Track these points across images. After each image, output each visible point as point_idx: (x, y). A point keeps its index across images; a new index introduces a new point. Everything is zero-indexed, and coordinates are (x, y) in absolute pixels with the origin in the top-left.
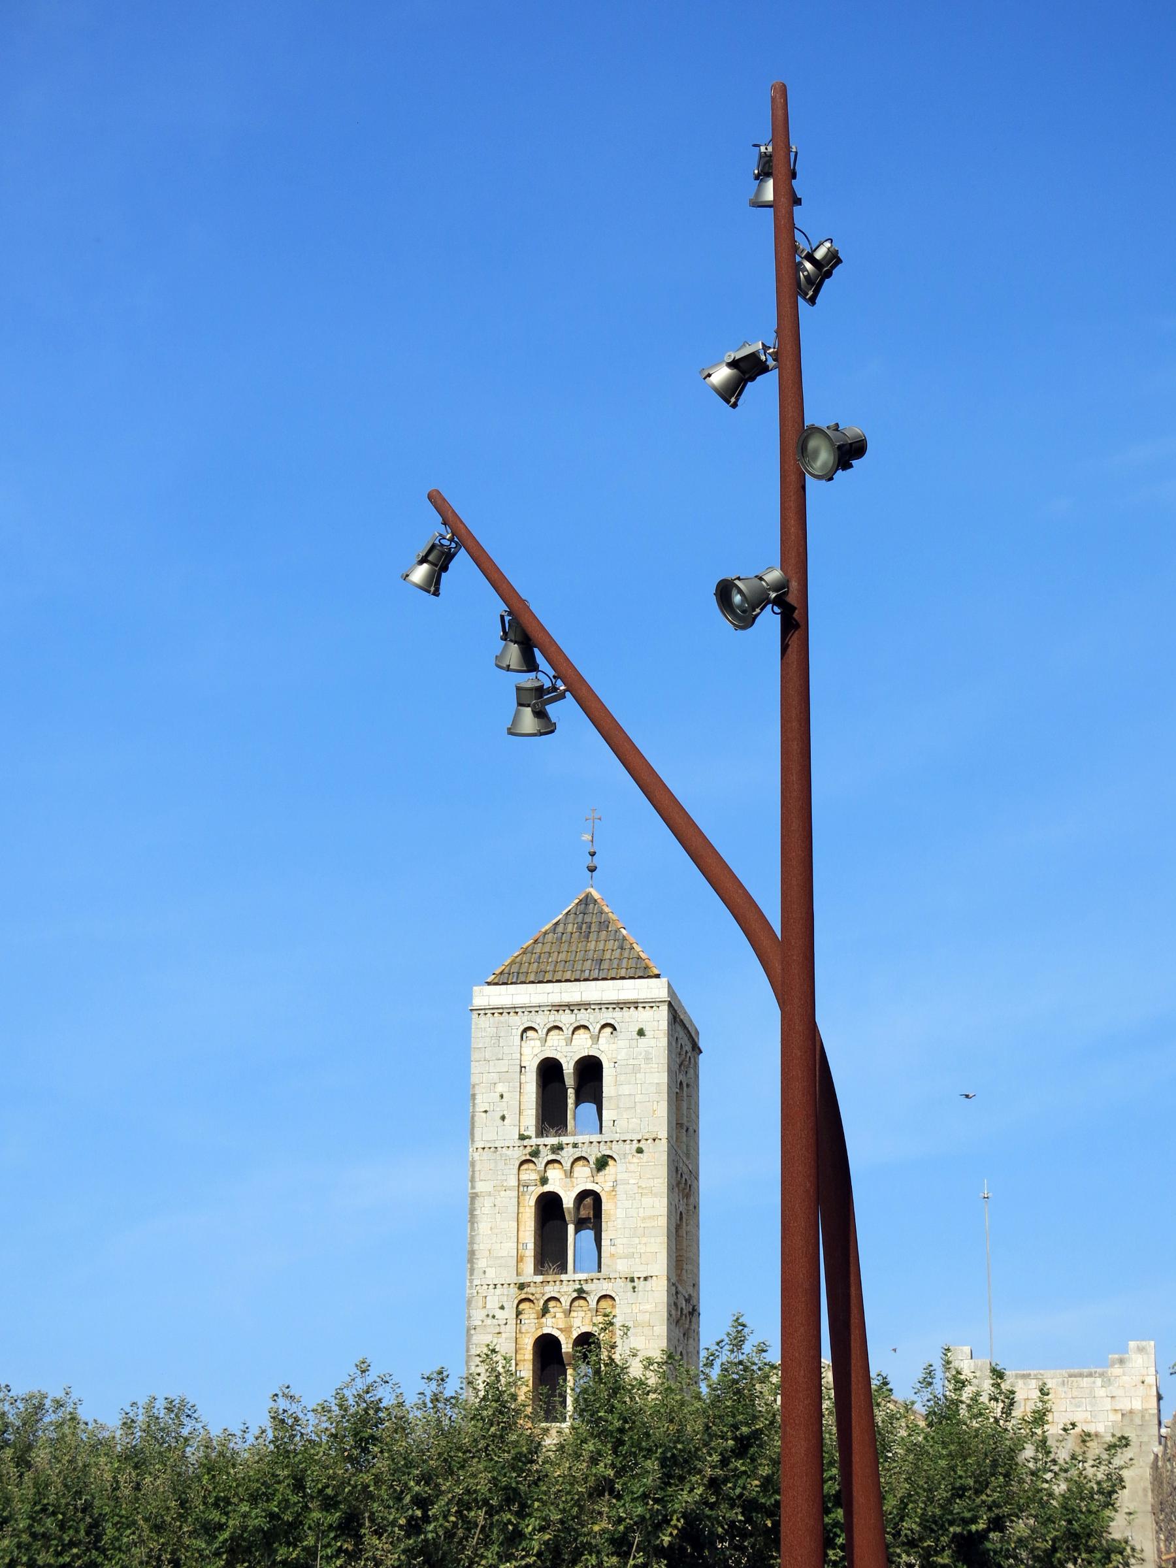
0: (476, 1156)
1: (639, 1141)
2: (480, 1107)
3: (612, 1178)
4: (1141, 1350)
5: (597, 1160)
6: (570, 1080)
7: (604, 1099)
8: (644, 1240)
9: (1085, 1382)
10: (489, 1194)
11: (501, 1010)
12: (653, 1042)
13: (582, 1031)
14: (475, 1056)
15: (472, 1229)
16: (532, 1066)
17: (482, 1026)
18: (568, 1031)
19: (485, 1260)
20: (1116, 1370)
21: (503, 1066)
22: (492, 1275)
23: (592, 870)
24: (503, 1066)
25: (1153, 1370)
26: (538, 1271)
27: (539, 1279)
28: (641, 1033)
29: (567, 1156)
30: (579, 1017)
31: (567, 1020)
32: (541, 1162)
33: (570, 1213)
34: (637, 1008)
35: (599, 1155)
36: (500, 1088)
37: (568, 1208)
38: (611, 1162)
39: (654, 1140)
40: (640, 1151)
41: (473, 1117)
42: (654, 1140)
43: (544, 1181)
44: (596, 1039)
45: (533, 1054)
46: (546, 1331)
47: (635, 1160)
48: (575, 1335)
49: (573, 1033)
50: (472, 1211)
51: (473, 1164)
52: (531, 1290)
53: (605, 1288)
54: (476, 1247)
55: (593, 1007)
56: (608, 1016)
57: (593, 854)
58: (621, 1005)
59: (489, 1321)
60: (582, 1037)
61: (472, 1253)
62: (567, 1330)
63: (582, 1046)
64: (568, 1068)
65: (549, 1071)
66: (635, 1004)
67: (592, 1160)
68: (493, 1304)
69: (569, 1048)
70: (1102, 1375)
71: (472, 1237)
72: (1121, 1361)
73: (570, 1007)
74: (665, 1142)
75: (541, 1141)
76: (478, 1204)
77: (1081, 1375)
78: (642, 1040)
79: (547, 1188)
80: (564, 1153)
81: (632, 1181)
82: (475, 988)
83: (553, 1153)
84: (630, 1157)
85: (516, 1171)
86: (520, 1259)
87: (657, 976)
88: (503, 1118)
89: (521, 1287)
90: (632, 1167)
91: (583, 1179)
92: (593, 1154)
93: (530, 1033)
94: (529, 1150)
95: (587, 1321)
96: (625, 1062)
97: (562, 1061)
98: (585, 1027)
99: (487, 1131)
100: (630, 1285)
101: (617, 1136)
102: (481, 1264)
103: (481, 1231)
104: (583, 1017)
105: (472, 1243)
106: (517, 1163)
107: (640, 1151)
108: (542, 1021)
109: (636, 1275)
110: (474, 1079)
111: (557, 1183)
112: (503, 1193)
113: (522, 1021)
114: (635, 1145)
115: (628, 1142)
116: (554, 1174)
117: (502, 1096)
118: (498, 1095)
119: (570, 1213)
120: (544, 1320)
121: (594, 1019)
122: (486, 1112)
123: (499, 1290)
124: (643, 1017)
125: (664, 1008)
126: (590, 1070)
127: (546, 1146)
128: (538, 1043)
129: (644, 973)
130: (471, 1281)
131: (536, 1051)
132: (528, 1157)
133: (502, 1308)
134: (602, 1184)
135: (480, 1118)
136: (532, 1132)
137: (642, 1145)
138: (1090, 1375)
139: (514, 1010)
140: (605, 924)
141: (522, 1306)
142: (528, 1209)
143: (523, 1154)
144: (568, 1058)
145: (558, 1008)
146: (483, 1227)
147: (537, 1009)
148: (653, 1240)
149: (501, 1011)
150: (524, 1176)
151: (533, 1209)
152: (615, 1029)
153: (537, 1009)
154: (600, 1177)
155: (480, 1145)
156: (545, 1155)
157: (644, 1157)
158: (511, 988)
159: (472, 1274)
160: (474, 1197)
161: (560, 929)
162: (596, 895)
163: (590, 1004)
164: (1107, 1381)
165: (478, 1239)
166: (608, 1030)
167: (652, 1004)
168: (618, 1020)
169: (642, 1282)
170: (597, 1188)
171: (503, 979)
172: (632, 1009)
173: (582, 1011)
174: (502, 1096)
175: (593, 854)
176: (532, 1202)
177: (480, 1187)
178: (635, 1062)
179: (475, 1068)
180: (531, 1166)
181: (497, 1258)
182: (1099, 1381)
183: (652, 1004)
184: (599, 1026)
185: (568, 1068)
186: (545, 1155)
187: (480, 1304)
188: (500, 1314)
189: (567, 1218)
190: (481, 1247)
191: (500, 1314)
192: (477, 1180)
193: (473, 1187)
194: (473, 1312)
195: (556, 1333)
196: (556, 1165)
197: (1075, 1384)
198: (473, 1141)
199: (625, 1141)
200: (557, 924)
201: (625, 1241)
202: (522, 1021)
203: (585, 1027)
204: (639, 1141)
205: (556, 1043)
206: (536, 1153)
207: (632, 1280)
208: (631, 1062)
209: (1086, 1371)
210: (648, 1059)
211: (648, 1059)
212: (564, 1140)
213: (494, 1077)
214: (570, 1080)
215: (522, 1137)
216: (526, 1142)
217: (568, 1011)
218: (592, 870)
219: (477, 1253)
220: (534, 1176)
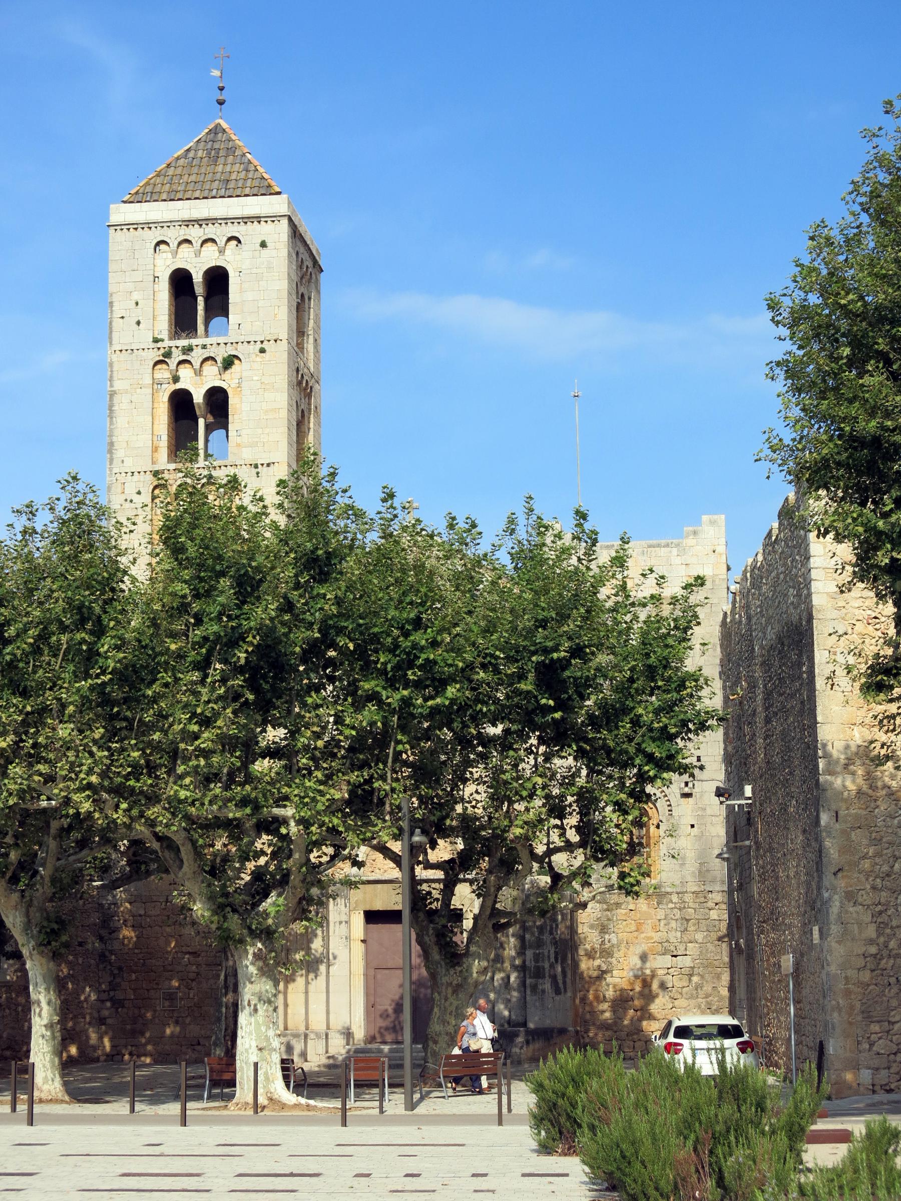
0: (115, 358)
1: (262, 342)
2: (117, 313)
4: (712, 523)
5: (224, 359)
7: (230, 305)
9: (663, 551)
10: (126, 392)
11: (135, 226)
13: (209, 244)
14: (112, 267)
15: (111, 423)
17: (118, 241)
18: (197, 244)
19: (123, 451)
20: (690, 541)
21: (138, 276)
22: (130, 464)
23: (221, 103)
24: (138, 276)
25: (723, 541)
26: (170, 460)
27: (172, 466)
28: (263, 245)
29: (196, 356)
31: (196, 234)
32: (173, 362)
34: (259, 222)
35: (226, 355)
36: (136, 296)
37: (198, 404)
38: (236, 362)
39: (276, 341)
40: (262, 351)
41: (111, 323)
42: (276, 341)
43: (176, 379)
44: (222, 251)
45: (165, 265)
47: (258, 359)
49: (202, 246)
50: (111, 408)
51: (111, 365)
54: (114, 439)
55: (219, 221)
57: (221, 89)
58: (246, 220)
59: (128, 505)
60: (210, 247)
61: (111, 444)
63: (210, 258)
64: (198, 278)
66: (258, 219)
67: (219, 359)
68: (130, 491)
69: (198, 259)
70: (678, 545)
71: (111, 430)
72: (695, 533)
73: (199, 222)
74: (285, 342)
75: (173, 343)
76: (116, 399)
77: (659, 546)
78: (265, 251)
79: (179, 386)
80: (193, 354)
81: (255, 378)
82: (112, 206)
83: (184, 354)
84: (254, 356)
85: (150, 370)
86: (155, 449)
87: (279, 193)
88: (138, 323)
89: (156, 474)
91: (212, 377)
92: (221, 354)
93: (163, 247)
94: (162, 351)
96: (249, 271)
98: (213, 241)
99: (123, 335)
100: (254, 471)
101: (242, 339)
102: (119, 454)
104: (210, 231)
105: (111, 436)
106: (152, 364)
107: (262, 351)
108: (173, 235)
109: (259, 462)
110: (112, 288)
111: (188, 381)
112: (139, 390)
113: (157, 235)
114: (259, 345)
115: (252, 343)
116: (185, 373)
117: (137, 304)
118: (134, 302)
119: (200, 407)
121: (220, 233)
122: (123, 317)
125: (285, 222)
127: (177, 347)
128: (170, 255)
129: (267, 190)
130: (111, 470)
131: (168, 262)
132: (161, 358)
133: (139, 493)
134: (228, 381)
135: (117, 324)
136: (165, 335)
137: (265, 345)
138: (667, 546)
140: (231, 150)
141: (157, 492)
142: (161, 405)
143: (157, 356)
144: (197, 269)
145: (188, 223)
146: (121, 421)
147: (169, 224)
149: (135, 226)
150: (158, 375)
151: (166, 405)
152: (239, 242)
153: (169, 224)
154: (227, 375)
156: (177, 356)
158: (145, 205)
159: (111, 463)
160: (112, 394)
161: (191, 154)
162: (225, 125)
163: (216, 219)
164: (683, 550)
165: (116, 433)
166: (234, 243)
167: (274, 218)
168: (243, 233)
169: (265, 468)
170: (224, 385)
171: (138, 198)
172: (256, 223)
173: (210, 225)
174: (137, 304)
176: (166, 398)
177: (118, 385)
178: (259, 271)
179: (112, 278)
180: (164, 366)
182: (675, 551)
183: (274, 218)
184: (225, 239)
186: (177, 356)
187: (119, 490)
188: (136, 498)
189: (198, 413)
190: (120, 439)
191: (136, 498)
192: (115, 378)
193: (111, 386)
194: (113, 498)
196: (187, 365)
197: (653, 554)
198: (111, 343)
199: (249, 342)
200: (188, 150)
202: (157, 235)
203: (213, 241)
204: (262, 342)
205: (186, 255)
206: (168, 354)
207: (256, 466)
208: (254, 271)
209: (663, 542)
210: (269, 268)
211: (269, 268)
212: (194, 342)
215: (156, 340)
216: (160, 345)
217: (197, 226)
218: (221, 103)
219: (115, 444)
220: (167, 375)
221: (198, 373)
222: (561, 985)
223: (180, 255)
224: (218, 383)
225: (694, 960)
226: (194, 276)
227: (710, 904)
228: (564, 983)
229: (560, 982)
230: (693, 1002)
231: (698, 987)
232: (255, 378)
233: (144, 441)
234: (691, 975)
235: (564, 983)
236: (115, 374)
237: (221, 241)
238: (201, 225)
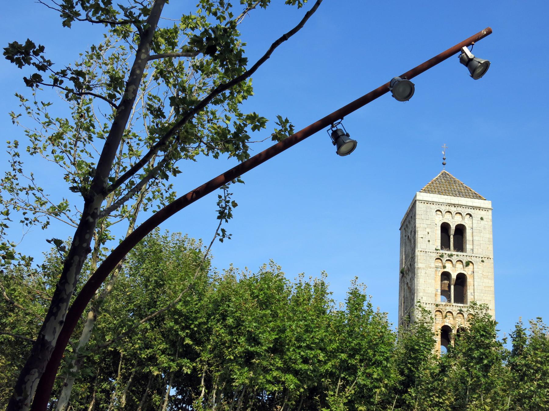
3: (472, 270)
5: (466, 262)
6: (452, 232)
8: (485, 295)
11: (428, 202)
12: (486, 223)
14: (417, 217)
21: (428, 222)
23: (444, 164)
24: (428, 222)
28: (482, 219)
30: (458, 209)
31: (453, 209)
33: (454, 281)
35: (467, 261)
36: (428, 230)
37: (454, 279)
38: (471, 264)
40: (483, 261)
43: (444, 267)
45: (439, 220)
46: (446, 324)
47: (481, 264)
52: (441, 307)
58: (474, 208)
60: (459, 216)
65: (445, 227)
66: (479, 208)
67: (464, 262)
73: (455, 205)
78: (482, 222)
79: (445, 270)
80: (453, 257)
81: (480, 272)
83: (449, 257)
86: (436, 295)
88: (429, 241)
89: (437, 305)
90: (480, 267)
93: (438, 212)
94: (439, 254)
96: (475, 228)
97: (451, 224)
101: (473, 255)
103: (420, 282)
104: (459, 210)
107: (483, 261)
111: (450, 269)
112: (429, 269)
114: (481, 259)
116: (449, 265)
117: (428, 233)
118: (427, 232)
120: (445, 320)
121: (464, 211)
122: (422, 238)
124: (482, 213)
126: (460, 230)
127: (445, 254)
132: (439, 257)
134: (467, 271)
136: (439, 248)
137: (483, 259)
139: (433, 203)
142: (438, 277)
143: (436, 256)
145: (450, 205)
147: (442, 204)
148: (489, 295)
154: (466, 269)
157: (484, 264)
158: (432, 195)
163: (462, 205)
166: (468, 216)
172: (478, 210)
174: (428, 233)
175: (444, 159)
176: (440, 274)
178: (480, 229)
180: (439, 261)
181: (427, 293)
184: (466, 214)
186: (446, 258)
199: (476, 257)
201: (478, 294)
204: (482, 258)
206: (442, 256)
210: (485, 228)
213: (425, 226)
214: (452, 232)
215: (436, 250)
216: (438, 251)
217: (453, 207)
221: (454, 266)
224: (462, 272)
226: (452, 226)
232: (480, 272)
237: (464, 214)
238: (455, 207)
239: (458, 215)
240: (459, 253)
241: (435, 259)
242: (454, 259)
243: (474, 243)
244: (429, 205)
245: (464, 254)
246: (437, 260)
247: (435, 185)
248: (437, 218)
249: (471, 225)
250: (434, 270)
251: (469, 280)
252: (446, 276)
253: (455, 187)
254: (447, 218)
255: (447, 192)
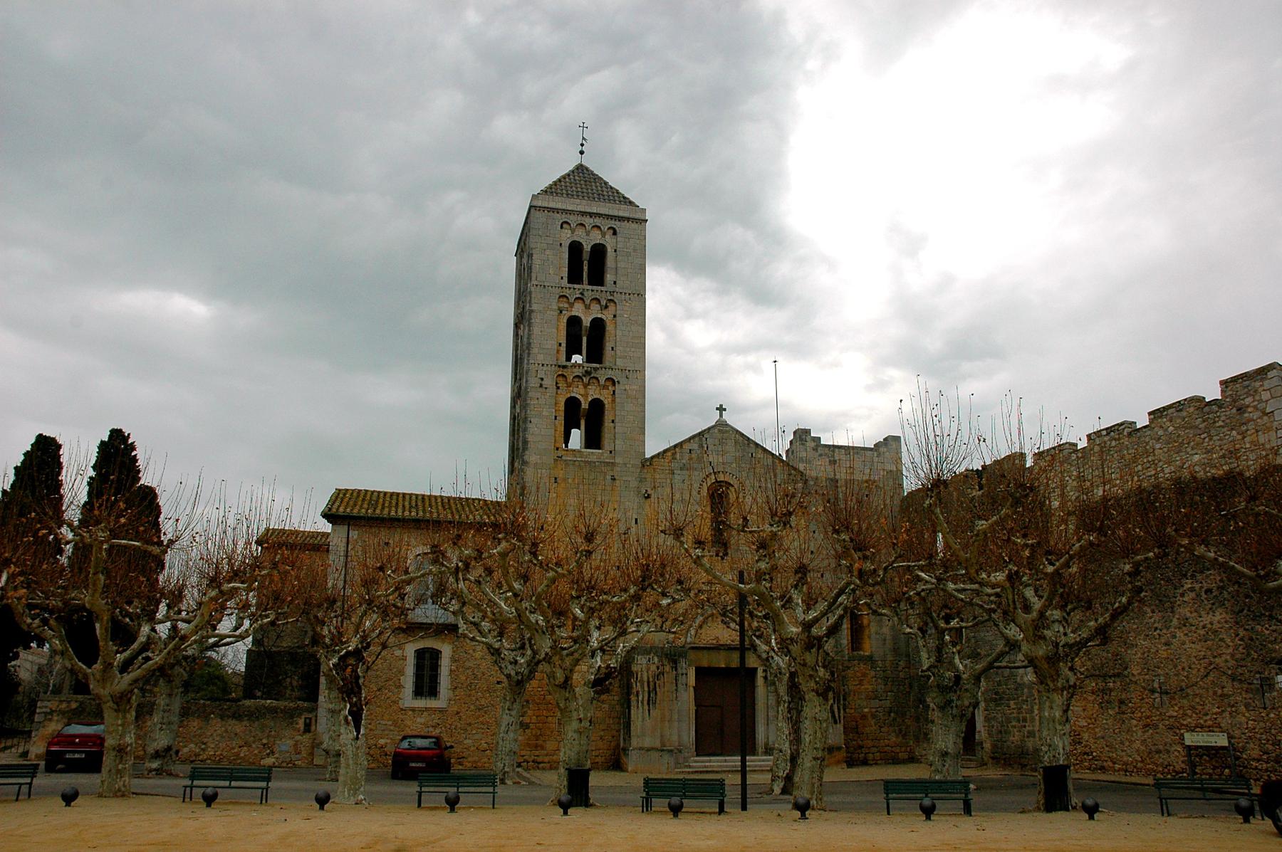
0: (533, 289)
6: (586, 256)
8: (633, 350)
16: (566, 244)
23: (582, 153)
31: (588, 221)
45: (566, 237)
48: (590, 399)
53: (610, 374)
56: (613, 223)
57: (582, 145)
58: (621, 219)
60: (597, 232)
62: (585, 396)
63: (596, 237)
64: (587, 248)
65: (575, 248)
73: (591, 215)
90: (626, 308)
93: (565, 226)
95: (597, 392)
97: (584, 244)
98: (599, 227)
102: (535, 350)
104: (598, 221)
113: (564, 218)
123: (545, 368)
126: (599, 252)
130: (528, 360)
134: (607, 316)
145: (583, 214)
147: (571, 212)
155: (535, 283)
159: (528, 356)
170: (604, 317)
175: (582, 145)
176: (565, 321)
180: (565, 299)
185: (587, 248)
189: (583, 332)
193: (530, 306)
195: (578, 396)
214: (586, 256)
218: (582, 153)
222: (837, 718)
223: (576, 233)
224: (599, 316)
225: (891, 703)
226: (585, 247)
227: (900, 668)
228: (839, 717)
229: (837, 715)
230: (891, 729)
231: (894, 719)
233: (551, 344)
234: (891, 712)
235: (839, 717)
236: (533, 300)
239: (595, 229)
240: (595, 288)
241: (558, 296)
242: (588, 296)
243: (619, 272)
244: (551, 214)
245: (603, 288)
246: (561, 299)
247: (563, 183)
248: (563, 235)
249: (615, 244)
250: (556, 313)
251: (610, 327)
252: (574, 322)
253: (594, 188)
254: (580, 236)
255: (580, 194)
